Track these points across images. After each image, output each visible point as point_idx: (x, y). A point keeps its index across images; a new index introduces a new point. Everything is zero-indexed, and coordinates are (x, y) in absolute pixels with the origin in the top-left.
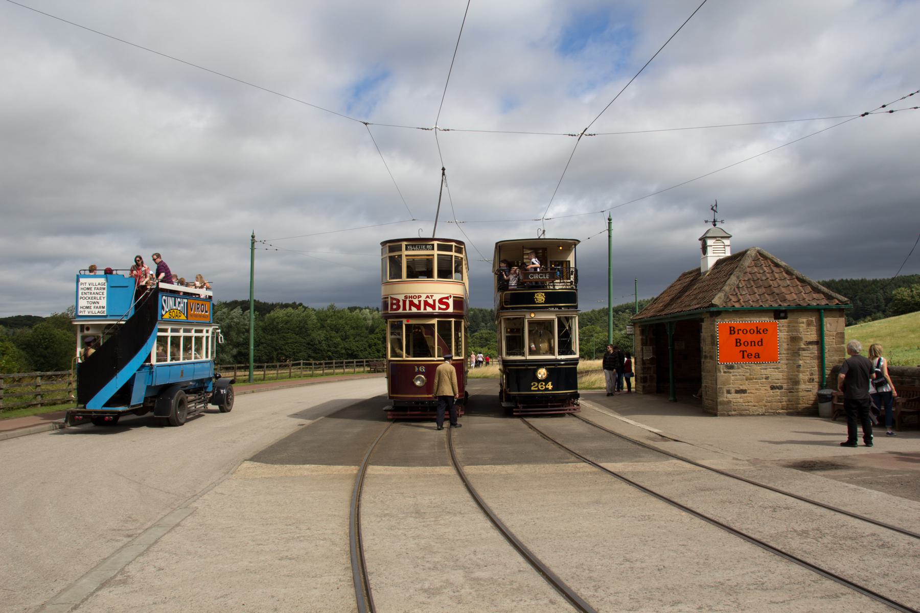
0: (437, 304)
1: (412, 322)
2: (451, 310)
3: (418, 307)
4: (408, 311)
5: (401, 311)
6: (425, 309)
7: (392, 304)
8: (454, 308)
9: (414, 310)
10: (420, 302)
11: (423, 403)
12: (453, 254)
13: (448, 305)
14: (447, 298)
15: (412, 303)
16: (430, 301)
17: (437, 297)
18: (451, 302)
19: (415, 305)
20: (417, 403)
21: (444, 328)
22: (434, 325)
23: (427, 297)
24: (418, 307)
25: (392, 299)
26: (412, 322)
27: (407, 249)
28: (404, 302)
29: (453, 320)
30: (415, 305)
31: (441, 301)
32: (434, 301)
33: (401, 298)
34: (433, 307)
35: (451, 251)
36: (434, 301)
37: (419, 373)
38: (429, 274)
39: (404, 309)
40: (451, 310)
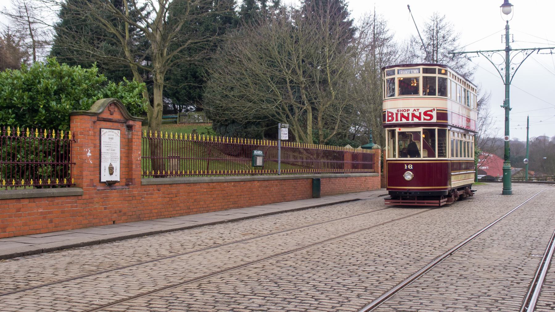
0: (423, 116)
1: (403, 130)
2: (434, 120)
3: (407, 119)
4: (399, 122)
5: (394, 122)
6: (413, 120)
7: (388, 116)
8: (437, 119)
9: (404, 121)
10: (408, 114)
11: (410, 193)
12: (437, 75)
13: (431, 117)
14: (431, 111)
15: (402, 116)
16: (417, 114)
17: (422, 111)
18: (434, 114)
19: (405, 117)
20: (406, 193)
21: (430, 134)
22: (420, 132)
23: (415, 110)
24: (407, 119)
25: (389, 112)
26: (403, 130)
27: (398, 73)
28: (397, 114)
29: (436, 128)
30: (405, 117)
31: (425, 114)
32: (420, 113)
33: (394, 111)
34: (419, 118)
35: (435, 73)
36: (420, 113)
37: (408, 170)
38: (415, 91)
39: (397, 120)
40: (434, 120)
